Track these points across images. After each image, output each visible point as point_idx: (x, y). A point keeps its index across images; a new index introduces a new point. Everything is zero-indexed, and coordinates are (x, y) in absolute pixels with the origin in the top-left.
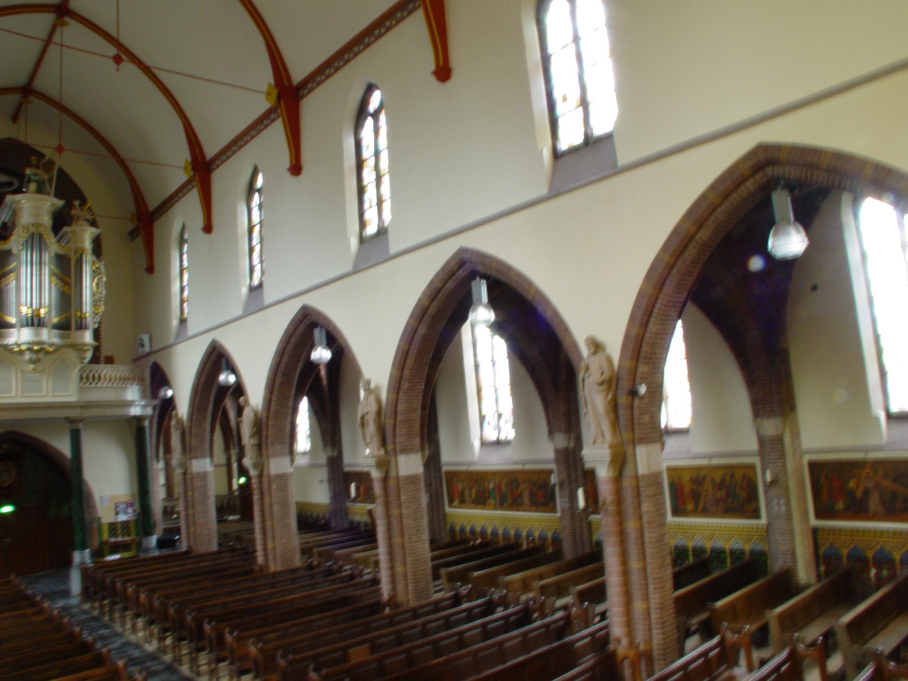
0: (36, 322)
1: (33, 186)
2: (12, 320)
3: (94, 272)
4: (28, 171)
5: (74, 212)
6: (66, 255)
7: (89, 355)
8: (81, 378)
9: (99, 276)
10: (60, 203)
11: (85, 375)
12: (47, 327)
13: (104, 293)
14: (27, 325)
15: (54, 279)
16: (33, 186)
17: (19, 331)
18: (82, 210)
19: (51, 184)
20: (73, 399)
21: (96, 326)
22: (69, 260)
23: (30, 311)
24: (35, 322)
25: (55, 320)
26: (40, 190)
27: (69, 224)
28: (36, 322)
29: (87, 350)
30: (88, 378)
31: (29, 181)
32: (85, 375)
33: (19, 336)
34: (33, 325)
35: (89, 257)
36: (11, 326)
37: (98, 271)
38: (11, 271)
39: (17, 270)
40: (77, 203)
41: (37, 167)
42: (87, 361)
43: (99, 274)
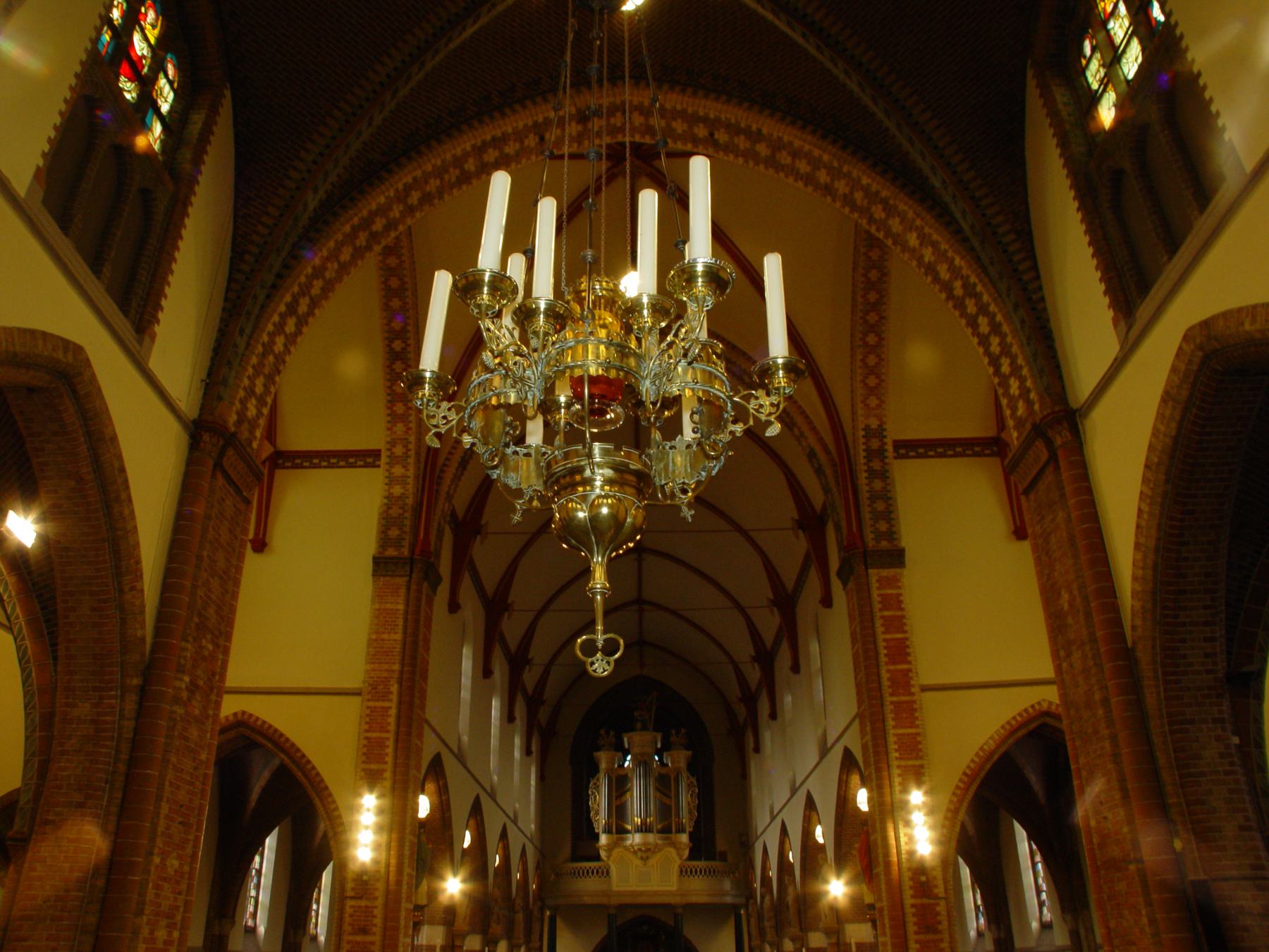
0: (644, 829)
1: (639, 725)
2: (629, 827)
3: (689, 785)
4: (636, 714)
5: (671, 739)
7: (686, 853)
8: (681, 871)
9: (692, 789)
11: (684, 869)
12: (653, 832)
14: (638, 831)
15: (658, 794)
16: (639, 725)
20: (674, 888)
22: (670, 778)
23: (639, 820)
24: (644, 829)
25: (659, 827)
26: (644, 728)
28: (644, 829)
29: (684, 849)
30: (686, 872)
33: (633, 840)
34: (642, 831)
35: (685, 774)
36: (628, 832)
38: (628, 790)
39: (631, 789)
40: (674, 732)
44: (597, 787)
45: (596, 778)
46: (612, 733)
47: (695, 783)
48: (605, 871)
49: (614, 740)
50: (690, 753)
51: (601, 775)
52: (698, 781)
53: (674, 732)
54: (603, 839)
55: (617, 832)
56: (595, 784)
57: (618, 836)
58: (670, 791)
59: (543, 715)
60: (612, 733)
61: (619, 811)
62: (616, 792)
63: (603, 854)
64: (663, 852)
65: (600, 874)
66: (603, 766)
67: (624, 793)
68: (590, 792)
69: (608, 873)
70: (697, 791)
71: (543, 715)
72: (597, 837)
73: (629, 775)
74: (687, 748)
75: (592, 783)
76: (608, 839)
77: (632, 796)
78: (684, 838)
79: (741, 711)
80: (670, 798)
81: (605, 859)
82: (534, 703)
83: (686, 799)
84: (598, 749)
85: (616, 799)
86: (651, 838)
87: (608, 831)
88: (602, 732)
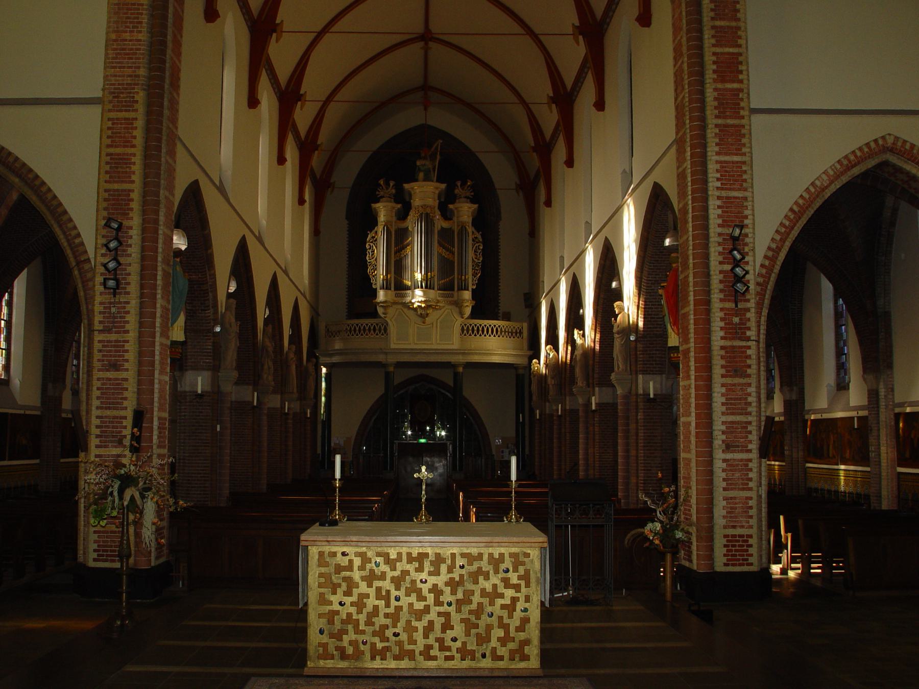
1: (421, 175)
3: (473, 240)
4: (418, 163)
5: (456, 191)
6: (451, 228)
7: (468, 311)
8: (463, 330)
10: (443, 186)
11: (465, 328)
13: (481, 259)
15: (442, 251)
16: (421, 175)
17: (413, 292)
18: (463, 189)
19: (434, 171)
21: (474, 287)
22: (453, 232)
26: (427, 179)
27: (453, 203)
30: (468, 330)
31: (420, 170)
32: (465, 328)
35: (470, 229)
36: (408, 288)
37: (477, 240)
40: (459, 183)
41: (425, 158)
42: (466, 316)
43: (477, 243)
44: (374, 240)
45: (374, 231)
46: (392, 183)
47: (481, 240)
48: (383, 328)
49: (394, 191)
50: (476, 206)
51: (380, 228)
52: (482, 236)
53: (459, 183)
54: (381, 296)
55: (396, 289)
56: (373, 237)
57: (396, 292)
58: (454, 247)
59: (317, 161)
60: (392, 183)
61: (397, 266)
62: (395, 246)
63: (380, 311)
64: (443, 310)
65: (377, 331)
66: (382, 218)
67: (404, 248)
68: (367, 247)
69: (385, 329)
70: (481, 248)
71: (317, 161)
72: (374, 293)
73: (410, 229)
74: (473, 201)
75: (369, 236)
76: (386, 295)
77: (412, 251)
78: (467, 295)
79: (533, 162)
80: (453, 254)
81: (383, 316)
82: (307, 147)
83: (472, 256)
84: (377, 201)
85: (396, 253)
86: (432, 293)
87: (386, 287)
88: (381, 182)
